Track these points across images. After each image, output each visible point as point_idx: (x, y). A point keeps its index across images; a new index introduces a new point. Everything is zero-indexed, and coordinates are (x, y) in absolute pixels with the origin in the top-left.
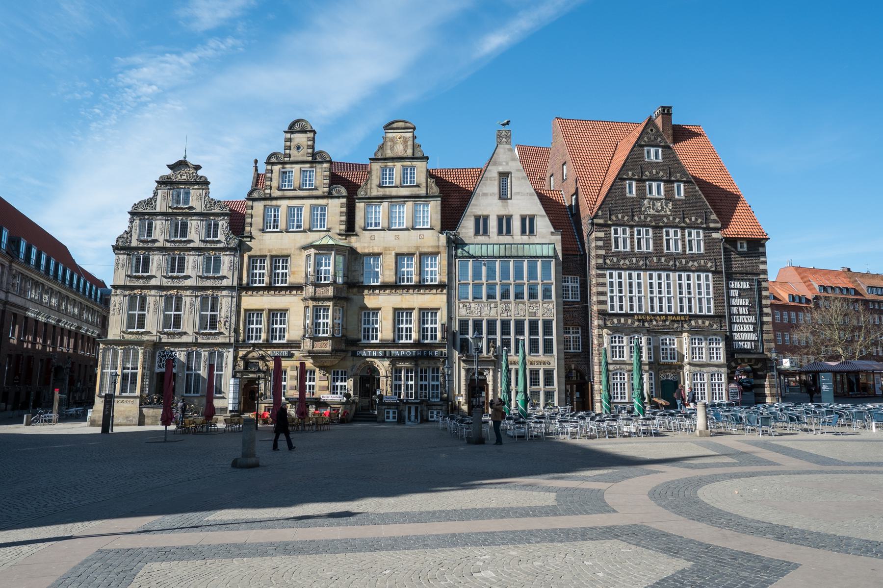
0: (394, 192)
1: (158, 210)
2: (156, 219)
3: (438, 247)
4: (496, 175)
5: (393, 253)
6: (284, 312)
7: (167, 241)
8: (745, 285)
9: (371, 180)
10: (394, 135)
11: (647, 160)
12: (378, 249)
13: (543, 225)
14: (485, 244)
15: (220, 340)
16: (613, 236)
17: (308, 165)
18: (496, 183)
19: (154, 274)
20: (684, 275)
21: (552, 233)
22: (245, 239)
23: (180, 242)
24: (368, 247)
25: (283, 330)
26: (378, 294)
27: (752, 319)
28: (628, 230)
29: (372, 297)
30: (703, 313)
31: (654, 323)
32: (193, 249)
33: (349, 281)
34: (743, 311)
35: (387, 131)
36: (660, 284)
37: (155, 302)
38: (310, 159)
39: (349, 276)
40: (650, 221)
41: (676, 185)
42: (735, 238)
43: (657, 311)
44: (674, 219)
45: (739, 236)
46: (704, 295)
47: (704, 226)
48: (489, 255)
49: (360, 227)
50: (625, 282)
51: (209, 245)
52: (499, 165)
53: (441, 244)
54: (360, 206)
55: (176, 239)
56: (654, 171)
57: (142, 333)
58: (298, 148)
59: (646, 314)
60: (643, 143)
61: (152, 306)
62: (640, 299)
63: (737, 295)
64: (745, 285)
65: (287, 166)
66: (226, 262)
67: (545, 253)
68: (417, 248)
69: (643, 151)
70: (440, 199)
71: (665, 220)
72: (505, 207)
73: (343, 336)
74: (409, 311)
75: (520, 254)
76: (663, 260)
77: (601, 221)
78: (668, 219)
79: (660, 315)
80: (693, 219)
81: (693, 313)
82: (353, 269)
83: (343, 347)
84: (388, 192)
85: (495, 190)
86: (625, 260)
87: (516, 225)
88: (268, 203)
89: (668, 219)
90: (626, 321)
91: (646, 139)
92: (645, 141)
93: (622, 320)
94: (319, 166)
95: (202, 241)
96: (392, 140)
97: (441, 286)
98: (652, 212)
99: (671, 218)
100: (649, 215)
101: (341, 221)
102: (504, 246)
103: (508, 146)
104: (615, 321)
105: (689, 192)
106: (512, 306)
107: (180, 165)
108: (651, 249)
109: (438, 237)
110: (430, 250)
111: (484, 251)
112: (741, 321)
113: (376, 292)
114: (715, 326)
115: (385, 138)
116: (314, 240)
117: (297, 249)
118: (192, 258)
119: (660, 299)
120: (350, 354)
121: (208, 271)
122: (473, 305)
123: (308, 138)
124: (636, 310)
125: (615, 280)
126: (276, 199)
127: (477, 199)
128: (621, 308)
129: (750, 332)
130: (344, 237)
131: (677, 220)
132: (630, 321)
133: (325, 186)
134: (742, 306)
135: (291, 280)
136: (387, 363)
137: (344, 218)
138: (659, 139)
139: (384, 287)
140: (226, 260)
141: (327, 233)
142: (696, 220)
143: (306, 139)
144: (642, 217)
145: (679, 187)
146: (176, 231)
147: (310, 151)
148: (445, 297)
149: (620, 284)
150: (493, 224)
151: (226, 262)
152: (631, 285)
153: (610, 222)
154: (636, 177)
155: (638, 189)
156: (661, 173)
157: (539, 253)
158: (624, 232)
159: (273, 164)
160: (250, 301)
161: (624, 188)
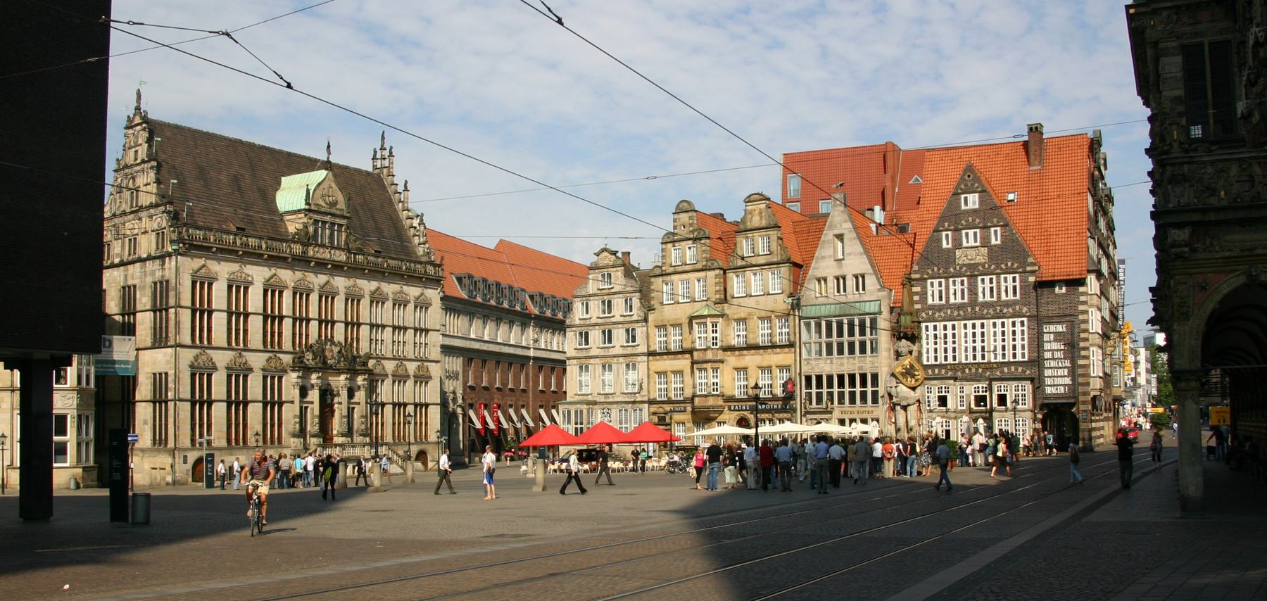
0: (754, 261)
1: (591, 293)
5: (755, 318)
7: (598, 318)
8: (1060, 328)
10: (752, 207)
11: (963, 207)
13: (871, 282)
14: (824, 305)
16: (929, 288)
17: (690, 242)
20: (999, 322)
21: (879, 290)
23: (607, 317)
25: (683, 389)
26: (745, 355)
27: (1067, 363)
28: (943, 280)
29: (741, 357)
30: (1017, 360)
31: (967, 371)
33: (724, 344)
34: (1057, 355)
36: (974, 335)
38: (692, 236)
40: (966, 271)
41: (992, 230)
42: (1052, 280)
43: (970, 360)
44: (990, 266)
45: (1056, 278)
46: (1019, 343)
47: (1021, 270)
50: (940, 334)
51: (628, 319)
54: (731, 275)
56: (970, 219)
59: (960, 363)
60: (959, 191)
62: (954, 350)
63: (1052, 339)
64: (1060, 328)
65: (677, 244)
67: (872, 310)
69: (960, 199)
71: (980, 268)
72: (840, 267)
74: (769, 368)
75: (852, 312)
76: (977, 309)
77: (917, 276)
78: (984, 267)
79: (972, 364)
80: (1009, 264)
81: (1006, 360)
85: (831, 252)
86: (940, 312)
87: (851, 283)
88: (668, 278)
89: (984, 267)
90: (940, 371)
91: (962, 186)
92: (961, 189)
93: (937, 371)
95: (621, 316)
96: (751, 212)
98: (967, 262)
99: (987, 266)
100: (964, 265)
104: (930, 371)
105: (1006, 236)
106: (845, 361)
108: (966, 300)
111: (824, 311)
112: (1056, 365)
113: (745, 352)
114: (1028, 372)
115: (745, 210)
119: (974, 349)
120: (726, 409)
121: (628, 342)
122: (813, 362)
123: (690, 217)
124: (950, 360)
125: (931, 332)
126: (670, 274)
127: (816, 262)
128: (936, 358)
129: (1066, 376)
130: (719, 305)
131: (993, 267)
132: (943, 371)
134: (1057, 350)
138: (976, 185)
142: (1012, 264)
143: (688, 219)
144: (958, 268)
145: (996, 231)
147: (691, 228)
148: (793, 355)
149: (935, 336)
151: (639, 333)
152: (945, 336)
153: (926, 276)
154: (952, 227)
155: (954, 240)
156: (978, 220)
157: (867, 311)
158: (940, 284)
161: (940, 240)
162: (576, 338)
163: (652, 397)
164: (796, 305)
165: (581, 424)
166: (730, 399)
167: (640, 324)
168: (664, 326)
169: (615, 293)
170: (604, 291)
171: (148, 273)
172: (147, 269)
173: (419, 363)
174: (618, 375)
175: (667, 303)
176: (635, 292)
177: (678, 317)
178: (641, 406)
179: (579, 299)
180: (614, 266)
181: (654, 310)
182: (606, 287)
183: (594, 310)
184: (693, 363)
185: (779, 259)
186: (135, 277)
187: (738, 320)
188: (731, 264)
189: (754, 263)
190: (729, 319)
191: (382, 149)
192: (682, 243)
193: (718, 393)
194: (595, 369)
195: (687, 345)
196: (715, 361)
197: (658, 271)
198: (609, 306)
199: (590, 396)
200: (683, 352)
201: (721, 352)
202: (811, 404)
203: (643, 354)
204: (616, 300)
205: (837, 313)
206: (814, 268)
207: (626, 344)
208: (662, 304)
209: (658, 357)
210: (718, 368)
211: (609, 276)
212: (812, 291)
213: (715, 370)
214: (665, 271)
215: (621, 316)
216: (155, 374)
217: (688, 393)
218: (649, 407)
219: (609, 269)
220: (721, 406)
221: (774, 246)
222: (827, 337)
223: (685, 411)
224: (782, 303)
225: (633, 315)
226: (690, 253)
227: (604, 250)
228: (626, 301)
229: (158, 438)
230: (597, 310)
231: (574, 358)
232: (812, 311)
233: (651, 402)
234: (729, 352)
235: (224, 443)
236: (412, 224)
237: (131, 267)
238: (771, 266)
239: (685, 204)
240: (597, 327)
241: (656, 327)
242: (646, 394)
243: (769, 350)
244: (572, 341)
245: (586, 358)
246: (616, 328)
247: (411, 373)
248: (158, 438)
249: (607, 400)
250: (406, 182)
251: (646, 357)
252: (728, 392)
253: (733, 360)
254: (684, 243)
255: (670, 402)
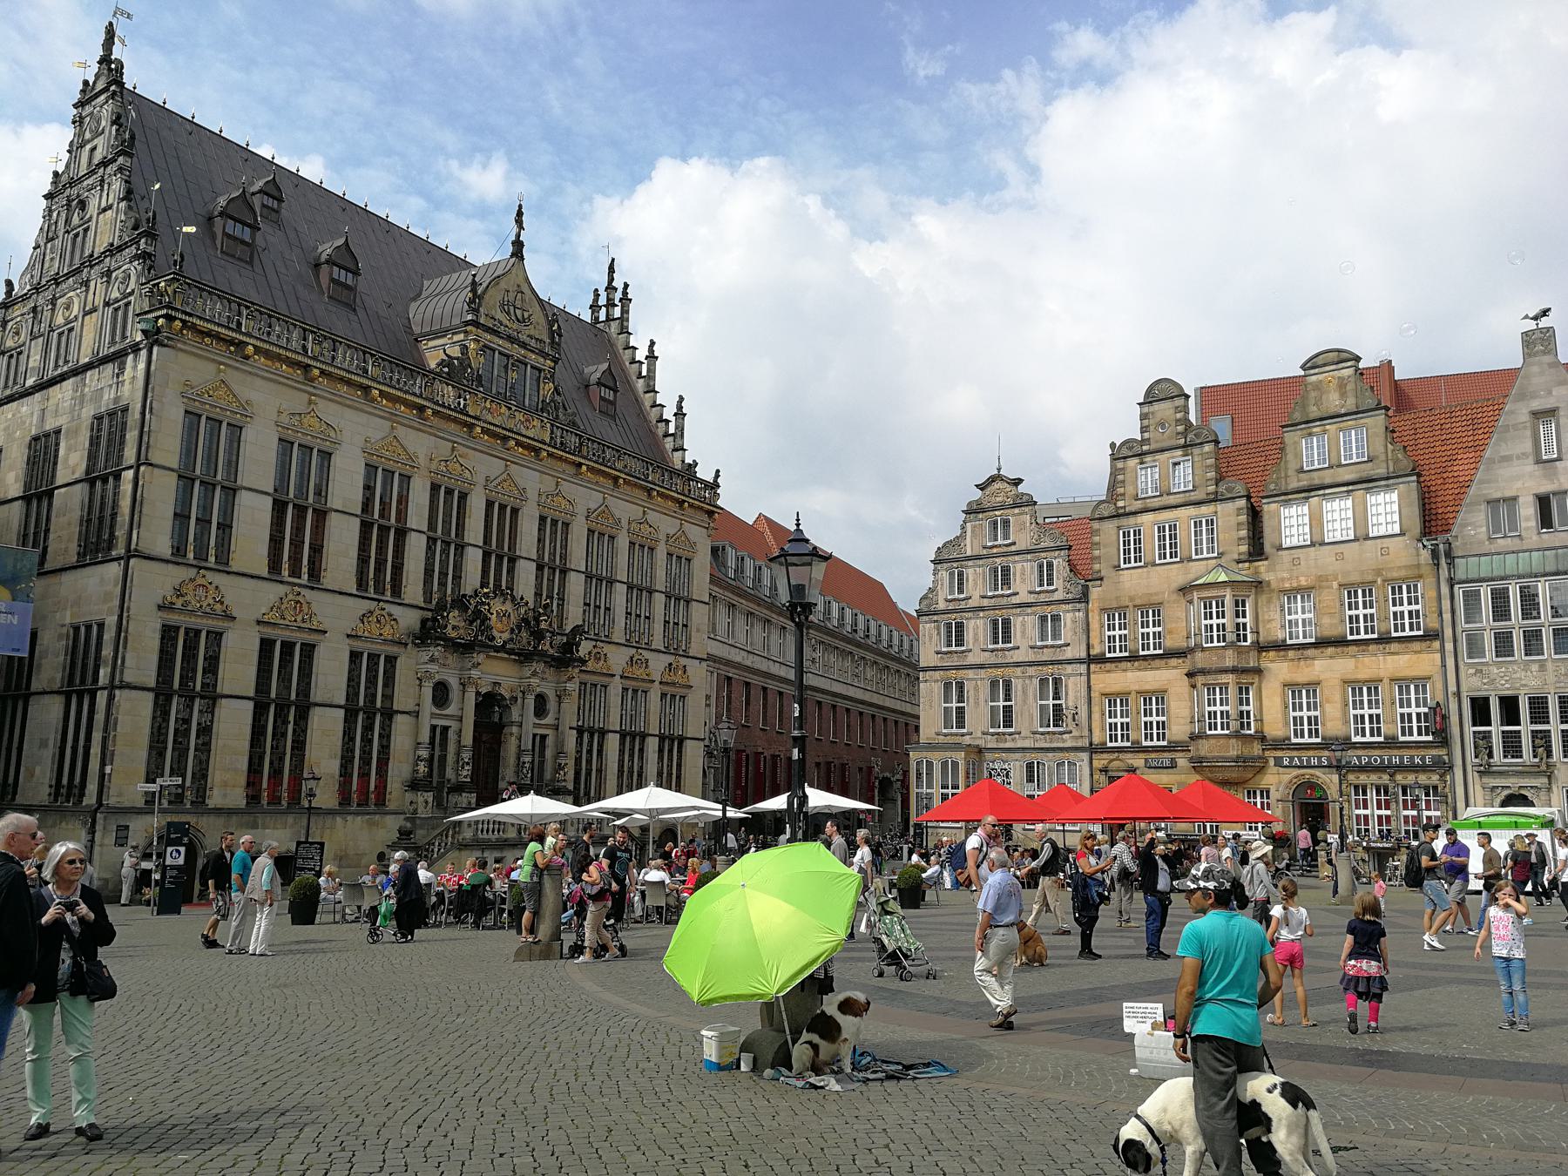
2: (967, 567)
3: (1418, 566)
4: (1523, 416)
5: (1335, 585)
6: (1161, 696)
7: (983, 597)
9: (1286, 462)
10: (1320, 377)
12: (1307, 581)
15: (1069, 744)
17: (1179, 452)
18: (1528, 433)
19: (971, 647)
22: (1090, 584)
23: (1003, 596)
24: (1288, 579)
26: (1313, 659)
29: (1302, 663)
32: (1020, 605)
35: (1308, 372)
37: (976, 688)
39: (1261, 630)
48: (1521, 571)
49: (1273, 546)
51: (1042, 598)
52: (1534, 396)
53: (1422, 562)
55: (996, 593)
57: (963, 735)
58: (1163, 425)
61: (972, 693)
65: (1148, 459)
66: (1069, 622)
68: (1378, 572)
70: (1414, 478)
73: (1256, 732)
74: (1373, 685)
82: (1266, 617)
83: (1256, 749)
84: (1317, 479)
85: (1528, 446)
88: (1124, 521)
94: (1196, 451)
95: (1031, 592)
96: (1318, 386)
97: (1431, 636)
101: (1240, 539)
102: (1554, 551)
103: (1547, 359)
107: (993, 481)
109: (1417, 549)
110: (1403, 573)
113: (1310, 652)
116: (1199, 574)
117: (1173, 592)
118: (1021, 618)
120: (1272, 762)
121: (1043, 637)
126: (1135, 513)
130: (1247, 565)
133: (1209, 483)
135: (1170, 642)
136: (1335, 778)
137: (1244, 533)
139: (1322, 643)
140: (1070, 619)
141: (1219, 561)
143: (1172, 411)
146: (997, 580)
147: (1180, 428)
150: (1528, 511)
151: (1069, 622)
159: (1125, 458)
160: (1109, 680)
162: (939, 634)
163: (1096, 740)
164: (1444, 556)
165: (955, 787)
166: (1282, 744)
167: (1070, 607)
168: (1122, 611)
169: (1018, 553)
170: (995, 550)
171: (88, 398)
172: (87, 390)
173: (671, 659)
174: (1024, 701)
175: (1128, 566)
176: (1059, 549)
177: (1152, 591)
178: (1072, 756)
179: (945, 566)
180: (1015, 506)
181: (1101, 579)
182: (999, 542)
183: (976, 584)
184: (1190, 675)
185: (1391, 469)
186: (61, 411)
187: (1292, 593)
188: (1272, 486)
189: (1328, 481)
190: (1273, 591)
191: (610, 288)
192: (1159, 456)
193: (1249, 732)
194: (976, 688)
195: (1174, 641)
196: (1245, 671)
197: (1107, 510)
198: (1004, 577)
199: (968, 737)
200: (1170, 654)
201: (1254, 654)
202: (1490, 755)
203: (1079, 661)
204: (1019, 566)
205: (1550, 568)
206: (1481, 482)
207: (1039, 644)
208: (1117, 567)
209: (1108, 665)
210: (1252, 684)
211: (1006, 523)
212: (1472, 526)
213: (1243, 689)
214: (1125, 507)
215: (1031, 592)
216: (76, 629)
217: (1179, 730)
218: (1091, 759)
219: (1006, 511)
220: (1260, 758)
221: (1379, 445)
222: (1526, 615)
223: (1173, 765)
224: (1407, 554)
225: (1057, 590)
226: (1185, 475)
227: (993, 479)
228: (1041, 566)
229: (65, 781)
230: (980, 582)
231: (935, 669)
232: (1485, 567)
233: (1093, 750)
234: (1272, 654)
235: (238, 798)
236: (662, 415)
237: (55, 391)
238: (1371, 485)
239: (1163, 385)
240: (981, 614)
241: (1103, 610)
242: (1086, 733)
243: (1372, 647)
244: (931, 638)
245: (958, 668)
246: (1019, 615)
247: (657, 677)
248: (65, 781)
249: (1002, 745)
250: (652, 343)
251: (1083, 668)
252: (1274, 730)
253: (1279, 670)
254: (1167, 455)
255: (1137, 749)
